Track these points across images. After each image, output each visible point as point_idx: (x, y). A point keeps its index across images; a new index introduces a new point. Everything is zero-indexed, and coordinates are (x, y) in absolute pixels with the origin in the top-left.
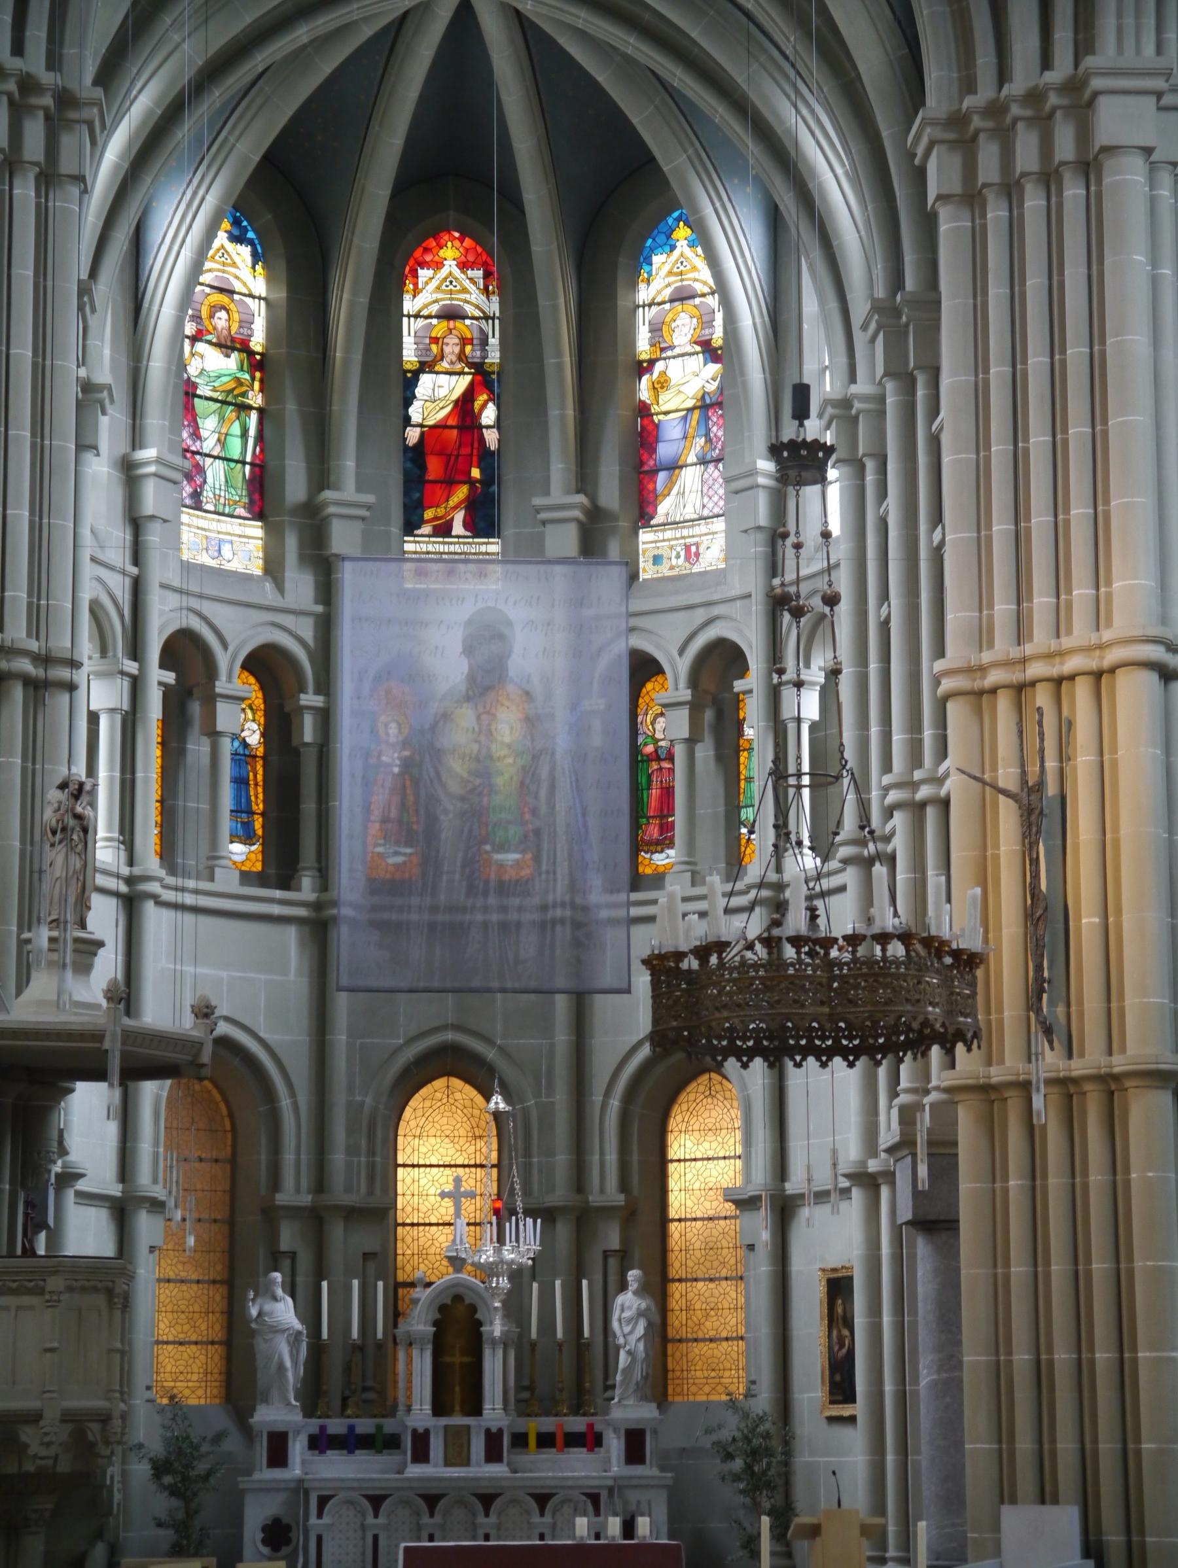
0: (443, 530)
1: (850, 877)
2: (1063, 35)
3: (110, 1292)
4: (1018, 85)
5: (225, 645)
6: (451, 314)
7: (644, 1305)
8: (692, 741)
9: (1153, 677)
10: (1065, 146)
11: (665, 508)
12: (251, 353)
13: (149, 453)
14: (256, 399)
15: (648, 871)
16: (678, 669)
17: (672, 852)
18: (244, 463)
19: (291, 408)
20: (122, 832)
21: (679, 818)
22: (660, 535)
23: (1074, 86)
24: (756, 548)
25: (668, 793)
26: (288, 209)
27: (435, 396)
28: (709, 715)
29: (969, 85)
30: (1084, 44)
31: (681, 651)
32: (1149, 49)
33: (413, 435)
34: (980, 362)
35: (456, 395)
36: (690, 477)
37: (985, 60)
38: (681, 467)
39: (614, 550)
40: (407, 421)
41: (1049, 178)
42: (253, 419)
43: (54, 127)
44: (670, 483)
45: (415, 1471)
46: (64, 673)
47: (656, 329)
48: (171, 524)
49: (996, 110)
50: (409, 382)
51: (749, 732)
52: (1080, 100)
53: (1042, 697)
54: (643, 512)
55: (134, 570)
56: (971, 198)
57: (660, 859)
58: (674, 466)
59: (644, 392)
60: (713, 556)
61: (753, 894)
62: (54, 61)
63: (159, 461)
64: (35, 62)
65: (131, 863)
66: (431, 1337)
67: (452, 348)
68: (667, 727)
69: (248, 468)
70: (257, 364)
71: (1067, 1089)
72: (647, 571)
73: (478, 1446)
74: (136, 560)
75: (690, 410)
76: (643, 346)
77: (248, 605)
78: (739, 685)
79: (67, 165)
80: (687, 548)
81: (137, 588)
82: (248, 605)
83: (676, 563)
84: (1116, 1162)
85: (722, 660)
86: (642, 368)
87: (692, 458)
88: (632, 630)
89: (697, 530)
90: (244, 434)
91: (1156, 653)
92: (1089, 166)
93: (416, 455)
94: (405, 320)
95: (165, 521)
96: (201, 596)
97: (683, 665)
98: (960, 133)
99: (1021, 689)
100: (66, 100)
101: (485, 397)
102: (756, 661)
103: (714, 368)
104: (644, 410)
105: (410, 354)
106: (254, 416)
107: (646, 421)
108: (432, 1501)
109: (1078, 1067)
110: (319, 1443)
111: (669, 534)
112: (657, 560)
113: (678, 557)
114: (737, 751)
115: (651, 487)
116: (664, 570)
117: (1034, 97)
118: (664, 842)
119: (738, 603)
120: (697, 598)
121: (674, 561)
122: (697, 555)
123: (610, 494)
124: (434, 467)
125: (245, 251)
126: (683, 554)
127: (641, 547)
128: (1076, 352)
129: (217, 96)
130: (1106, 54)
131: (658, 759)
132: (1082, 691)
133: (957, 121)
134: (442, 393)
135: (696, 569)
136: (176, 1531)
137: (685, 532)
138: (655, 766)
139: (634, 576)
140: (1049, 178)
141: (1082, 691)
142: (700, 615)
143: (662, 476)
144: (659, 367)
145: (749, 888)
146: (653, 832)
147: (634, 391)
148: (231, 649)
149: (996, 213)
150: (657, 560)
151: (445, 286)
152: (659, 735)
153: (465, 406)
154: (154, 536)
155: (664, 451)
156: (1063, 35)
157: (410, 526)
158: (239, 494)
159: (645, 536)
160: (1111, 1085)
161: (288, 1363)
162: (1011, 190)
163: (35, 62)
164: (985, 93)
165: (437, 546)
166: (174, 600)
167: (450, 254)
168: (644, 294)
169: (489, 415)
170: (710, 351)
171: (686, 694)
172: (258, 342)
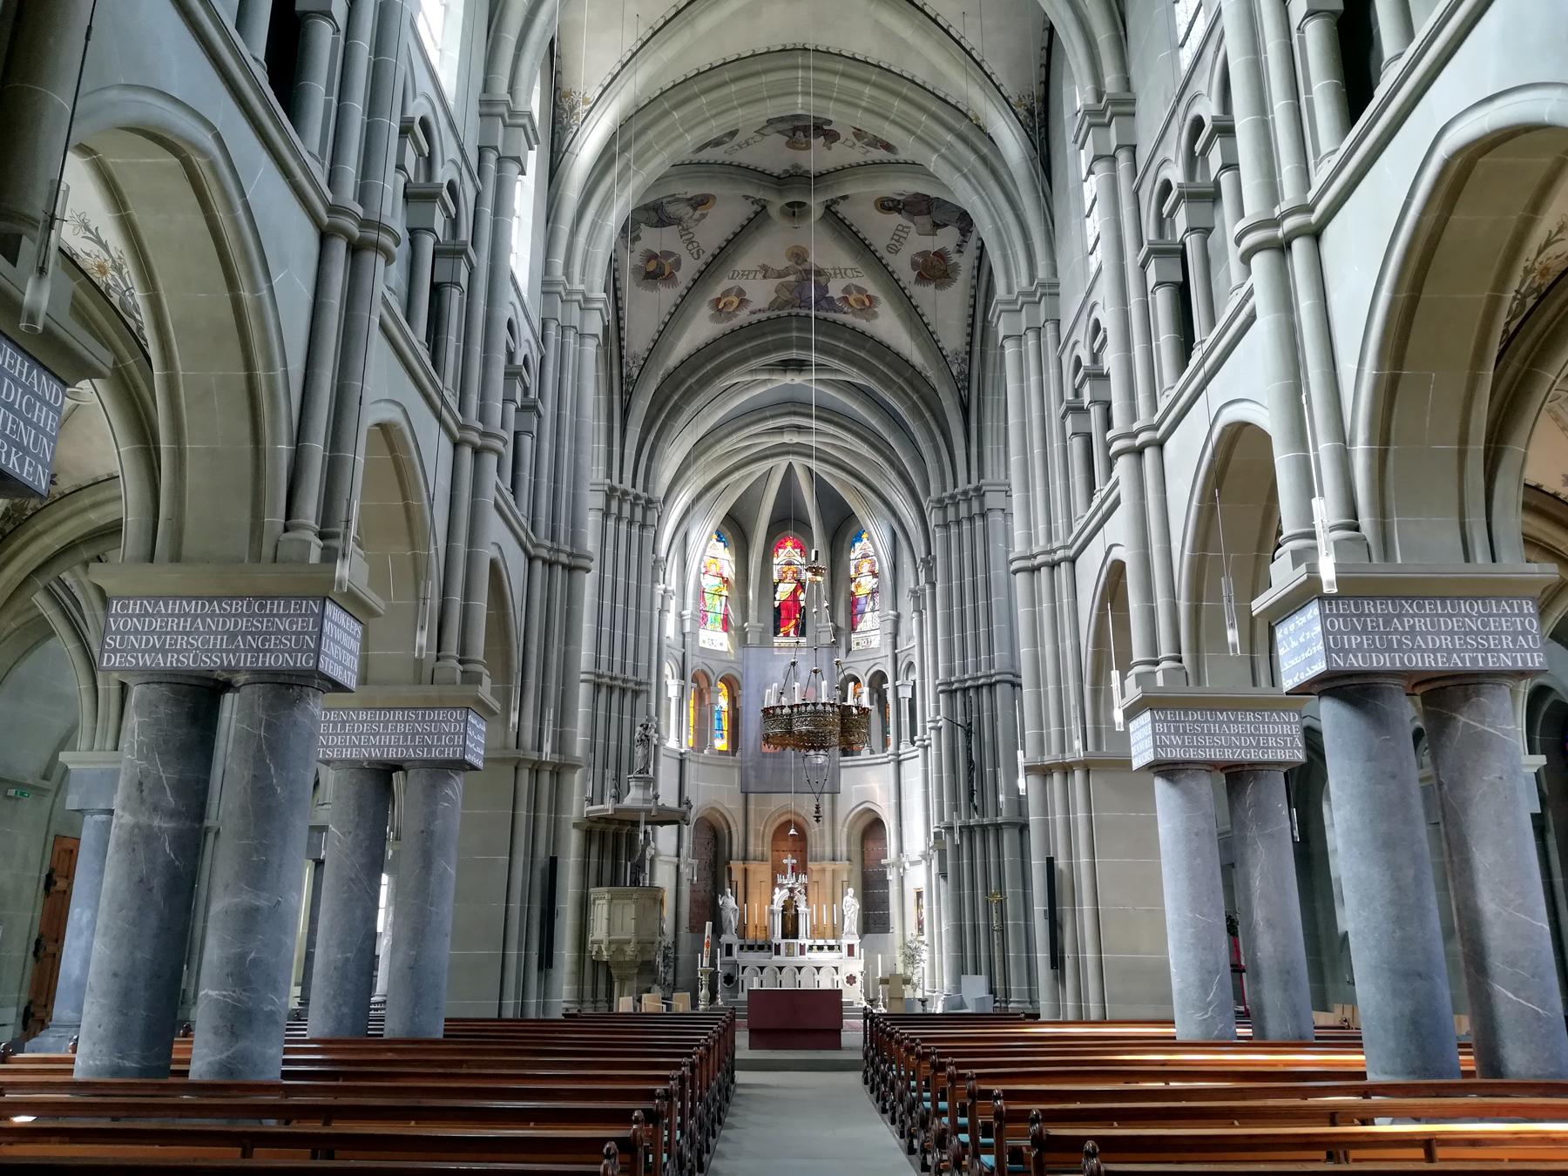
0: (787, 635)
1: (920, 752)
2: (974, 473)
3: (655, 899)
4: (960, 489)
6: (789, 564)
9: (1008, 686)
10: (976, 508)
11: (860, 627)
14: (725, 593)
16: (865, 680)
19: (736, 595)
23: (978, 489)
24: (889, 640)
26: (735, 528)
27: (784, 591)
29: (944, 489)
30: (981, 476)
32: (1002, 477)
33: (777, 604)
34: (949, 579)
36: (868, 616)
37: (949, 480)
39: (843, 640)
41: (971, 519)
43: (645, 509)
45: (775, 958)
46: (643, 687)
47: (857, 567)
48: (695, 635)
49: (952, 497)
50: (776, 587)
52: (980, 493)
53: (972, 693)
54: (853, 629)
56: (946, 526)
58: (863, 613)
62: (645, 489)
64: (639, 490)
67: (790, 575)
70: (726, 581)
71: (984, 828)
73: (797, 950)
79: (649, 522)
84: (999, 855)
85: (880, 677)
86: (852, 580)
91: (1010, 677)
92: (983, 515)
93: (778, 611)
97: (867, 679)
98: (941, 505)
99: (965, 690)
100: (649, 501)
104: (852, 594)
105: (776, 577)
109: (986, 821)
117: (965, 493)
123: (842, 621)
124: (784, 614)
128: (980, 576)
129: (709, 496)
130: (988, 477)
132: (985, 691)
133: (940, 501)
136: (648, 991)
139: (849, 650)
140: (971, 519)
141: (985, 691)
149: (954, 530)
151: (787, 554)
153: (794, 593)
154: (688, 639)
155: (859, 607)
156: (974, 473)
157: (776, 634)
158: (719, 626)
160: (998, 828)
162: (959, 523)
163: (639, 490)
164: (950, 490)
165: (786, 640)
166: (696, 660)
167: (789, 544)
168: (853, 556)
169: (802, 596)
170: (874, 575)
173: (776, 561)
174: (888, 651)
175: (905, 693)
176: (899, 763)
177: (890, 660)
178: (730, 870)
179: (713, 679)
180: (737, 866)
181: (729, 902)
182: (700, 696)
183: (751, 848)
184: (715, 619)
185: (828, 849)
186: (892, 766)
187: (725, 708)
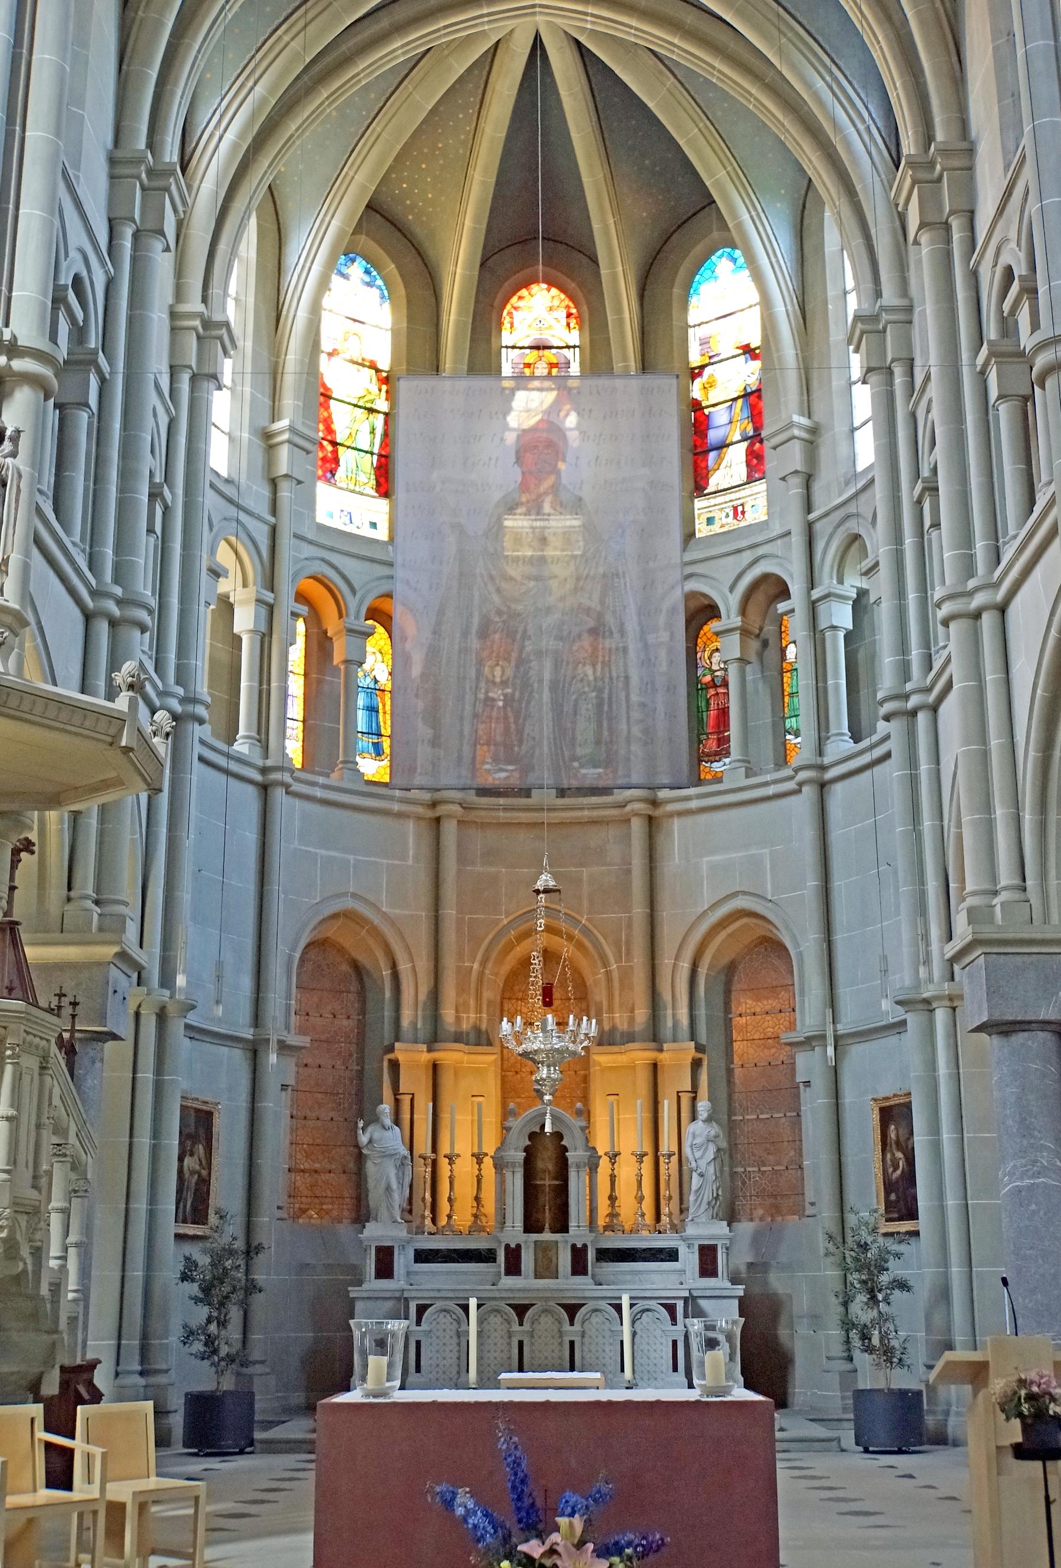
5: (354, 592)
7: (713, 1133)
8: (743, 661)
11: (715, 481)
12: (378, 371)
13: (283, 423)
14: (383, 405)
15: (709, 777)
16: (729, 603)
17: (727, 760)
18: (372, 454)
20: (259, 732)
21: (734, 731)
22: (712, 502)
25: (724, 712)
28: (754, 645)
31: (732, 589)
35: (545, 406)
38: (728, 446)
40: (506, 427)
42: (379, 421)
44: (719, 460)
45: (509, 1282)
47: (704, 342)
51: (791, 652)
55: (272, 520)
57: (717, 767)
58: (722, 446)
59: (696, 391)
60: (757, 510)
61: (803, 775)
63: (292, 429)
65: (266, 755)
66: (522, 1161)
68: (723, 651)
69: (375, 457)
70: (386, 380)
72: (702, 530)
73: (565, 1260)
74: (274, 511)
75: (734, 400)
76: (695, 359)
77: (372, 560)
78: (782, 607)
80: (735, 509)
81: (274, 531)
82: (372, 560)
83: (725, 522)
86: (695, 373)
87: (737, 437)
88: (690, 576)
89: (742, 494)
90: (373, 431)
94: (504, 350)
95: (299, 482)
96: (332, 549)
101: (568, 407)
102: (796, 587)
103: (757, 364)
104: (696, 406)
106: (381, 418)
107: (698, 413)
108: (521, 1310)
110: (423, 1256)
111: (720, 499)
112: (710, 521)
113: (727, 516)
114: (782, 673)
115: (703, 465)
116: (716, 529)
118: (723, 751)
119: (779, 542)
120: (744, 543)
121: (724, 521)
122: (743, 513)
125: (375, 292)
126: (731, 514)
127: (696, 512)
131: (715, 686)
134: (533, 405)
135: (743, 524)
137: (733, 496)
138: (712, 692)
139: (689, 536)
142: (747, 557)
143: (712, 455)
144: (708, 371)
145: (796, 771)
146: (712, 745)
147: (688, 391)
148: (358, 595)
150: (710, 521)
152: (715, 667)
158: (367, 479)
159: (699, 503)
161: (394, 1185)
166: (308, 551)
169: (571, 421)
171: (737, 621)
172: (385, 364)
173: (507, 338)
174: (794, 522)
175: (842, 616)
176: (823, 786)
177: (797, 540)
178: (395, 1065)
179: (352, 603)
180: (412, 1057)
181: (384, 1138)
182: (320, 647)
183: (448, 1014)
184: (357, 466)
185: (642, 1015)
186: (804, 803)
187: (383, 676)
